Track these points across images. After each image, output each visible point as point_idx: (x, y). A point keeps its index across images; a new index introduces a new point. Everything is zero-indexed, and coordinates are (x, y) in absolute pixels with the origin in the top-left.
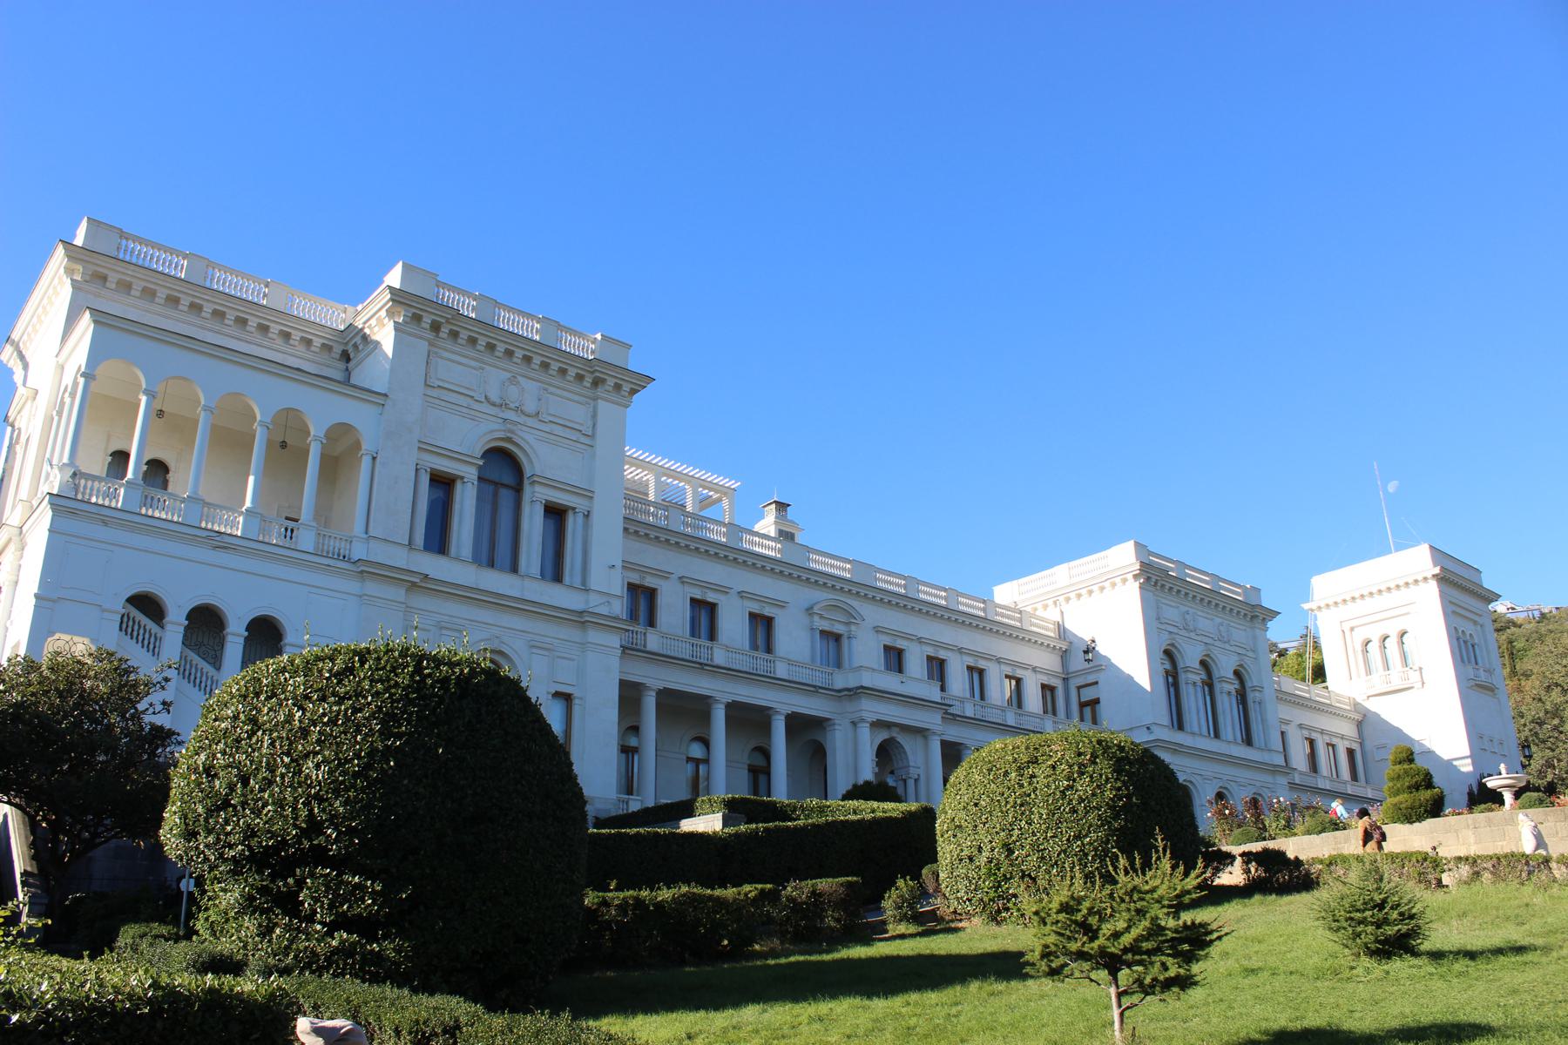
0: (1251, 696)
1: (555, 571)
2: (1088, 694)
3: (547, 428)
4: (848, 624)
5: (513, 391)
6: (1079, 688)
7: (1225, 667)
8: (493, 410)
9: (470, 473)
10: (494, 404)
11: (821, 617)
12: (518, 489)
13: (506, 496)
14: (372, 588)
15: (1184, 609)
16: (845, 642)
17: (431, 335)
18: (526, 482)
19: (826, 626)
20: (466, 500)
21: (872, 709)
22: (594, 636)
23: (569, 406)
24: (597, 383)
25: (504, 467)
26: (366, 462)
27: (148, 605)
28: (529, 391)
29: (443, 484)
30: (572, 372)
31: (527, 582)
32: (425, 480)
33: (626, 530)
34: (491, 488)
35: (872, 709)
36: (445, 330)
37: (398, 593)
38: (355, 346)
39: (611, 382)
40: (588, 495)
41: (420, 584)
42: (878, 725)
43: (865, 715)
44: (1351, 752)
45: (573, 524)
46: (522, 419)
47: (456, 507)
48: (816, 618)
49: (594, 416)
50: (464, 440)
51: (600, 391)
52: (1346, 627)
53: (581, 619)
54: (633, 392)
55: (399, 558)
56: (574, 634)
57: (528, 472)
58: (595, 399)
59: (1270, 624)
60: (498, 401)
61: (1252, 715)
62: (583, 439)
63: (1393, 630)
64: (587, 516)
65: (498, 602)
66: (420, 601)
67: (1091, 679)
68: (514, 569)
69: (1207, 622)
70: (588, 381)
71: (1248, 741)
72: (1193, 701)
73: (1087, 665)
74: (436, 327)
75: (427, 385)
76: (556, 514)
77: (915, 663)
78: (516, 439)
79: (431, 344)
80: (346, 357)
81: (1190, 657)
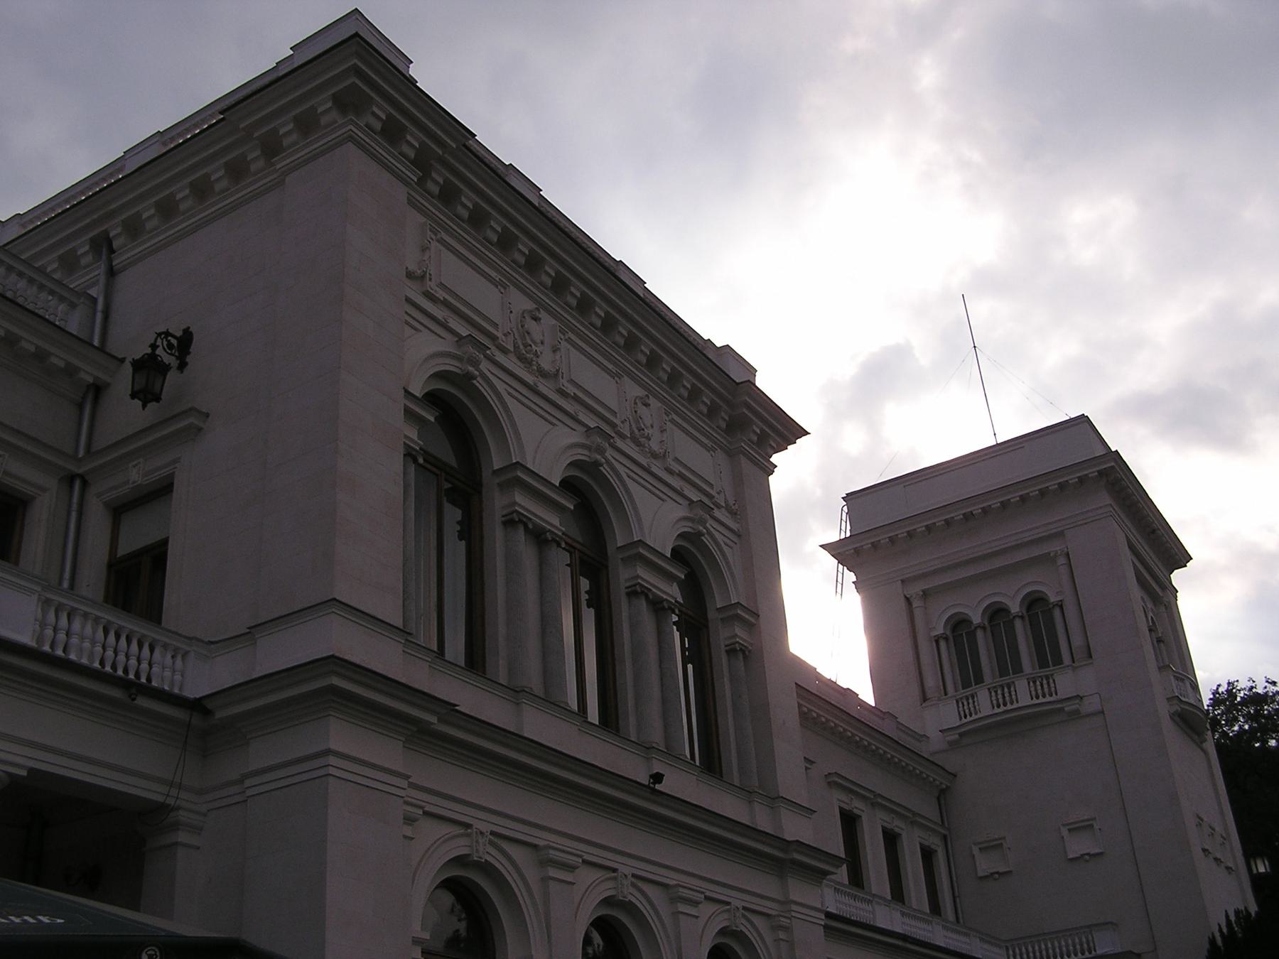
0: (721, 636)
52: (915, 589)
59: (775, 459)
61: (725, 688)
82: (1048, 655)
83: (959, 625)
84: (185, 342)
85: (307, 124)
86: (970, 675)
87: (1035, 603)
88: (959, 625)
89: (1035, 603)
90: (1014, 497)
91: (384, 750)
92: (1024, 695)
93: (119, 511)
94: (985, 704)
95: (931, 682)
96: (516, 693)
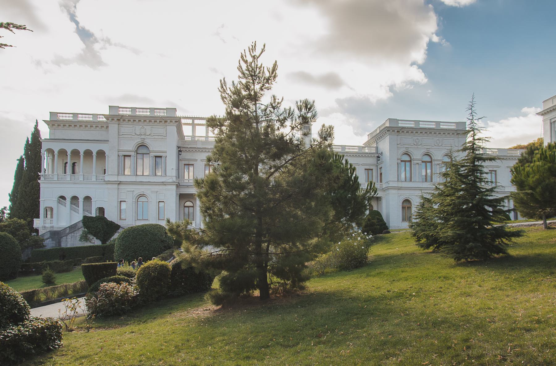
3: (153, 137)
9: (132, 154)
23: (159, 130)
25: (142, 148)
26: (107, 157)
27: (63, 198)
28: (148, 129)
36: (121, 120)
37: (116, 186)
41: (120, 183)
50: (130, 146)
51: (167, 124)
53: (163, 184)
55: (115, 178)
65: (142, 183)
66: (122, 187)
70: (163, 121)
74: (119, 120)
75: (119, 135)
81: (417, 155)
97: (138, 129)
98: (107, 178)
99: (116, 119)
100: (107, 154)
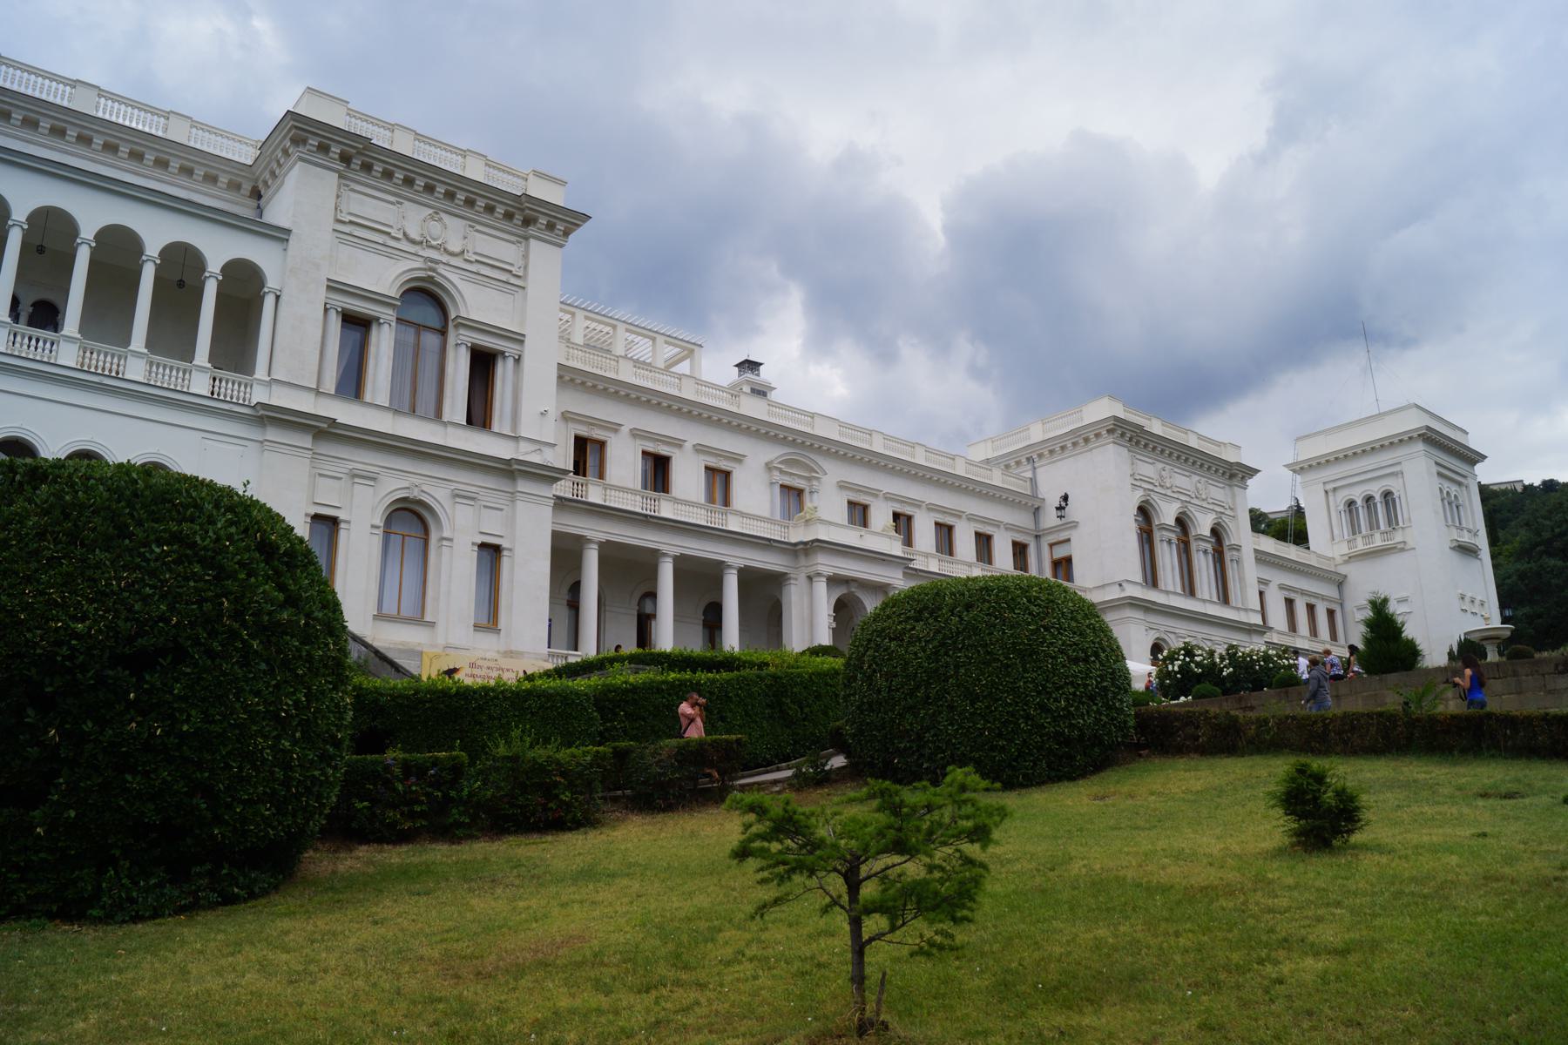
0: (1228, 556)
1: (479, 415)
2: (1060, 553)
3: (473, 268)
4: (809, 479)
5: (435, 228)
6: (1051, 545)
7: (1203, 524)
8: (411, 248)
10: (413, 242)
11: (781, 471)
12: (443, 332)
13: (431, 340)
14: (273, 434)
15: (1160, 465)
16: (806, 495)
17: (341, 167)
18: (451, 324)
19: (788, 481)
20: (383, 344)
21: (828, 565)
22: (523, 486)
24: (527, 222)
26: (269, 302)
28: (453, 232)
29: (357, 324)
30: (500, 210)
31: (450, 429)
32: (335, 323)
33: (560, 377)
34: (412, 331)
35: (828, 565)
36: (357, 162)
37: (306, 441)
38: (265, 183)
39: (543, 221)
40: (519, 339)
41: (325, 431)
42: (834, 581)
43: (820, 568)
44: (1331, 613)
45: (503, 371)
46: (445, 258)
47: (372, 349)
48: (776, 473)
49: (526, 257)
50: (383, 276)
51: (532, 230)
52: (1330, 487)
53: (509, 470)
54: (566, 234)
56: (503, 484)
57: (453, 315)
58: (526, 238)
59: (1249, 482)
60: (418, 238)
62: (513, 280)
63: (1376, 490)
64: (518, 361)
66: (328, 449)
67: (1063, 536)
68: (438, 414)
69: (1184, 481)
70: (518, 219)
71: (1225, 599)
72: (1167, 559)
73: (1059, 522)
74: (345, 159)
76: (483, 363)
77: (881, 516)
78: (439, 279)
79: (341, 177)
80: (257, 194)
81: (1167, 514)
82: (1392, 520)
83: (1351, 504)
84: (1065, 498)
85: (1097, 435)
86: (1355, 529)
87: (1387, 495)
88: (1351, 504)
89: (1387, 495)
90: (1377, 445)
91: (1139, 615)
92: (1378, 541)
93: (1051, 545)
94: (1360, 545)
95: (1336, 532)
96: (1167, 592)
97: (412, 217)
98: (259, 395)
99: (336, 149)
100: (272, 282)
